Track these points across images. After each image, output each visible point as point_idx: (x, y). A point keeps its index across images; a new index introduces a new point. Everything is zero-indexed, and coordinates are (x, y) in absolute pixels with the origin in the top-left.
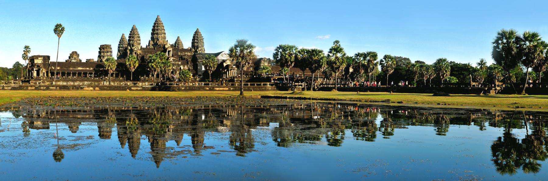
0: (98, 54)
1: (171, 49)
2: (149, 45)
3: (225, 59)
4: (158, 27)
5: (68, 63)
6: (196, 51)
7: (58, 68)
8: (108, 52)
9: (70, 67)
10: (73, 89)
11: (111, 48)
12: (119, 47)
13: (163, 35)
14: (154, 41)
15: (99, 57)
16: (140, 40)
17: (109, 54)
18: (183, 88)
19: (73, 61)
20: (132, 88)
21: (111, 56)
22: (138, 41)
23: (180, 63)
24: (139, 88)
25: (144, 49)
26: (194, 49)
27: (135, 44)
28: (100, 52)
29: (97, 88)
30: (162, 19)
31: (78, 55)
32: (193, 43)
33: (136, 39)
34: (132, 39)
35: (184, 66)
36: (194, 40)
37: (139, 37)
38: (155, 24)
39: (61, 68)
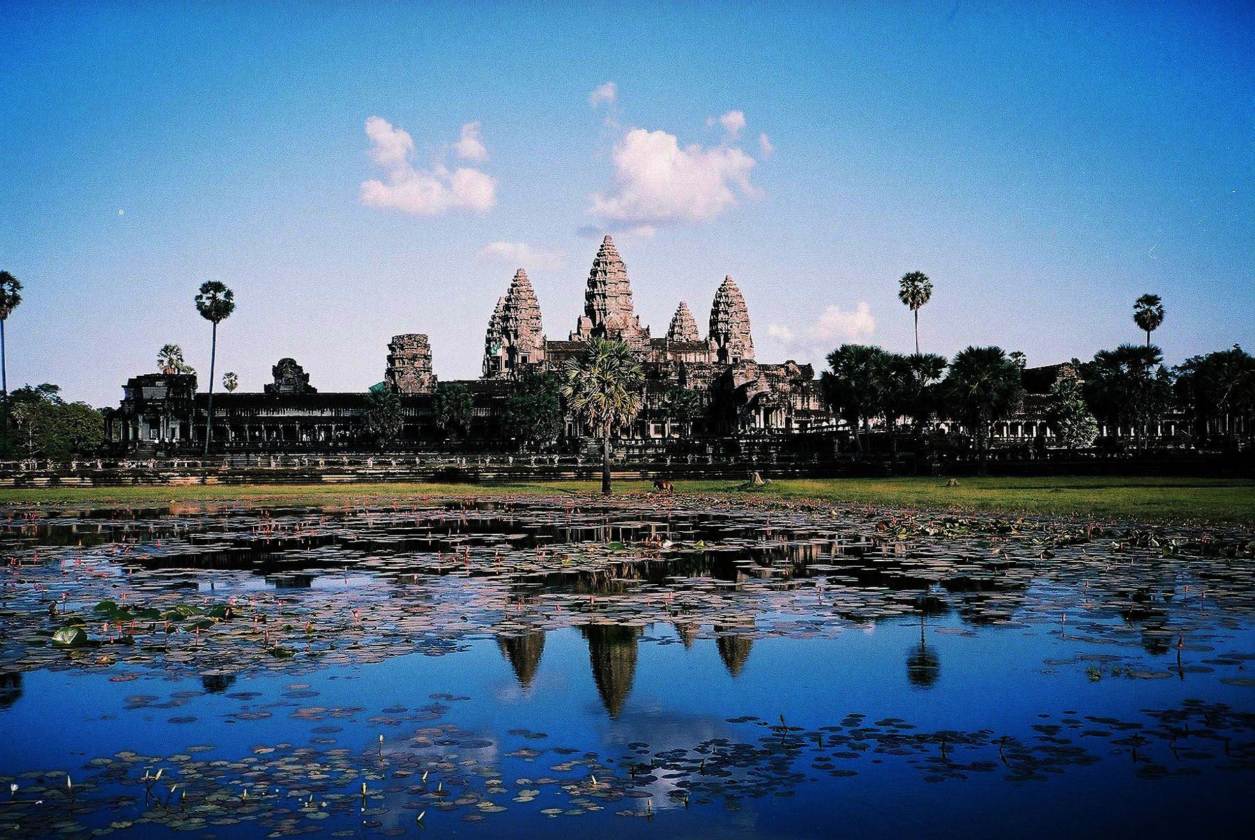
0: (384, 365)
2: (579, 333)
5: (270, 397)
6: (723, 353)
8: (415, 358)
10: (135, 482)
11: (427, 346)
14: (594, 322)
15: (390, 373)
17: (419, 364)
18: (491, 475)
20: (325, 478)
21: (429, 370)
25: (552, 345)
26: (718, 341)
27: (524, 329)
28: (391, 359)
30: (623, 246)
32: (713, 323)
33: (524, 315)
36: (715, 312)
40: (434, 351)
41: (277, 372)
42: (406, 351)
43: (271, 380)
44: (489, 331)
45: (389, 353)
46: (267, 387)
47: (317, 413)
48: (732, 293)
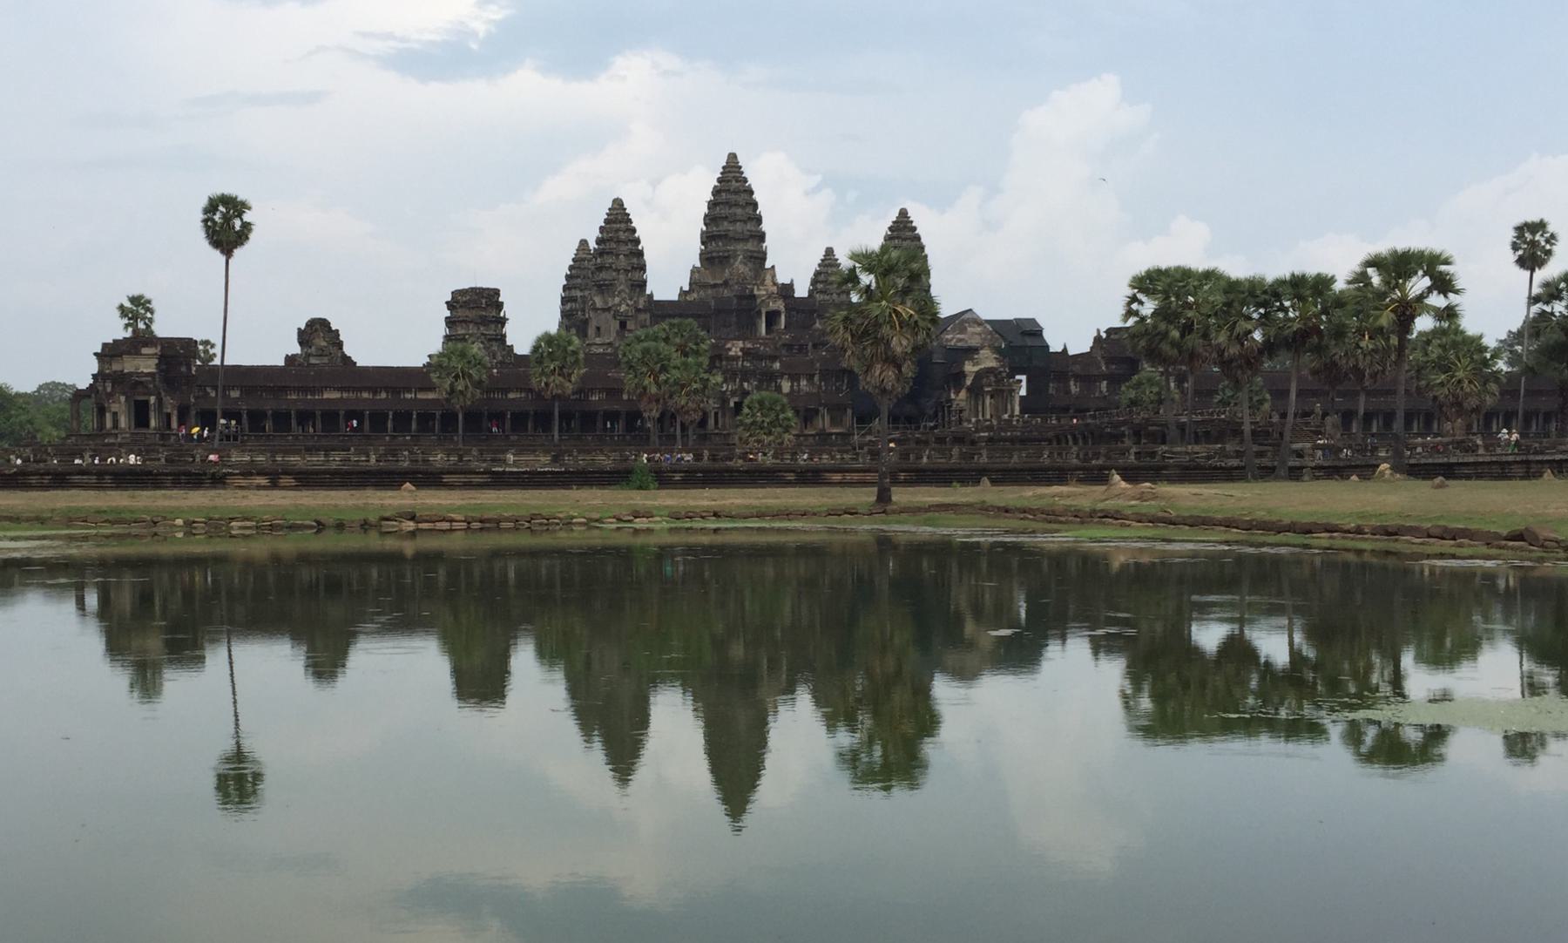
0: (441, 330)
1: (779, 305)
3: (975, 342)
4: (727, 204)
7: (235, 394)
9: (284, 389)
11: (500, 306)
12: (564, 301)
13: (750, 246)
16: (643, 268)
18: (678, 477)
19: (313, 361)
20: (447, 479)
22: (636, 275)
23: (777, 365)
24: (477, 479)
28: (450, 322)
29: (286, 480)
31: (334, 339)
34: (609, 260)
35: (794, 378)
37: (641, 254)
38: (716, 192)
39: (248, 391)
40: (507, 311)
41: (304, 337)
42: (476, 310)
43: (297, 349)
44: (565, 288)
45: (448, 313)
46: (290, 359)
47: (365, 395)
48: (909, 234)
